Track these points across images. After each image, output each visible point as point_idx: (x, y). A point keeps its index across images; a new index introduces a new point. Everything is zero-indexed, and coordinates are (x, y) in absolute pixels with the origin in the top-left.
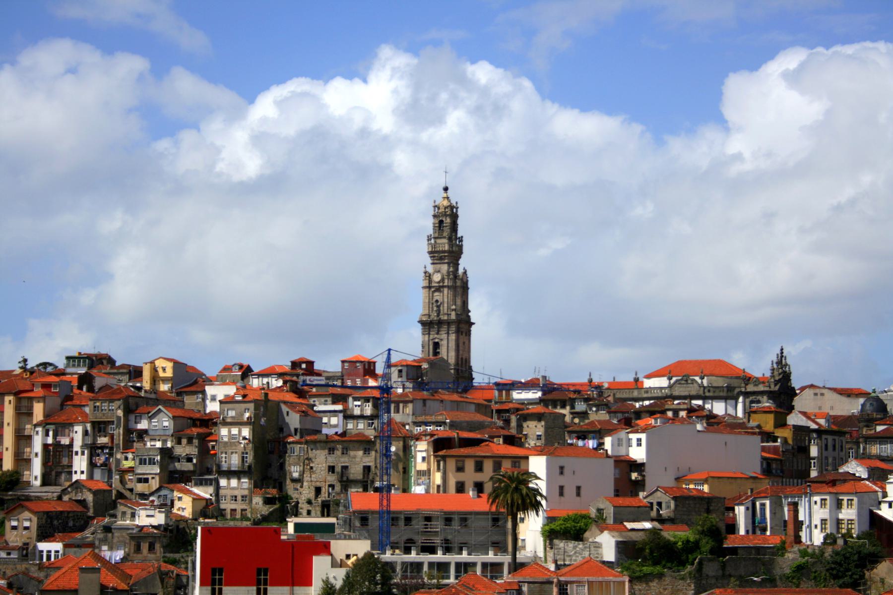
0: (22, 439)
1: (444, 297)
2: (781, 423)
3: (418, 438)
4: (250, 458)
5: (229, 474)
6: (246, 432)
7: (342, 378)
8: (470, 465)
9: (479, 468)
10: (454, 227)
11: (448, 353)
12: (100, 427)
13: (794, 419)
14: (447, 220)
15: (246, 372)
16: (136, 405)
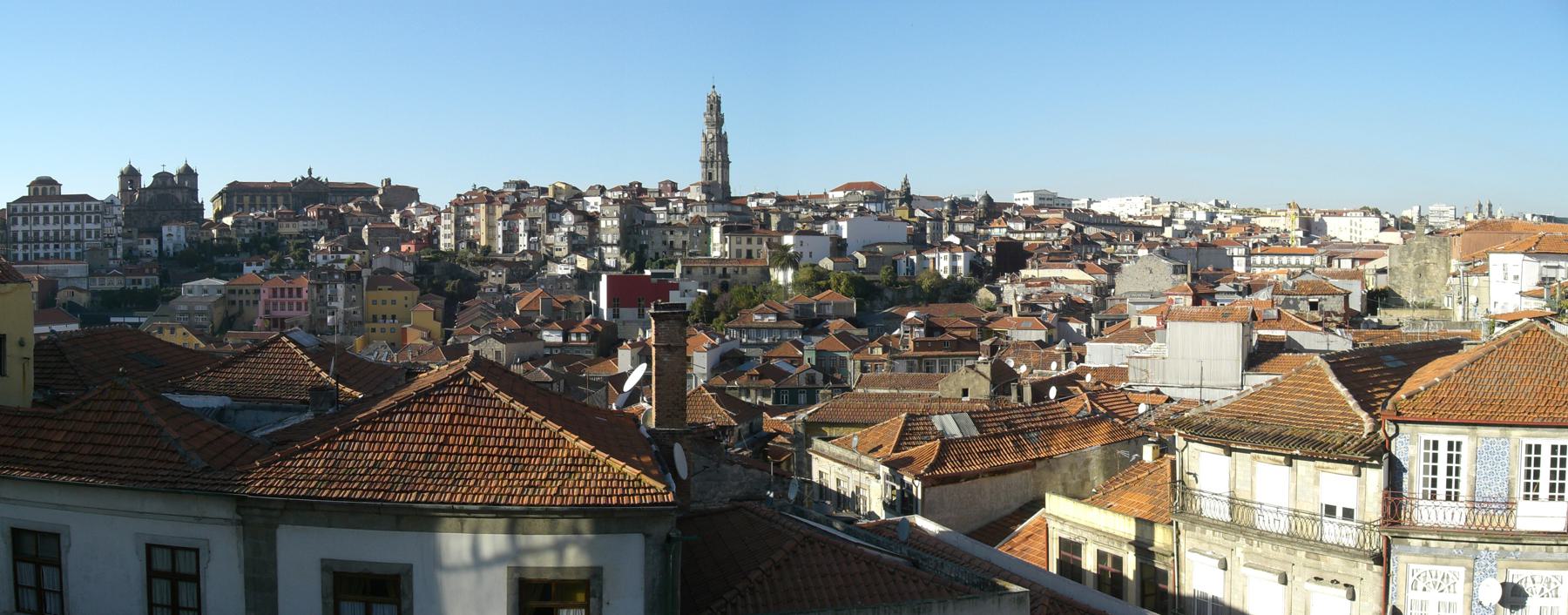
0: (490, 227)
1: (714, 147)
2: (912, 215)
3: (714, 224)
4: (618, 237)
5: (607, 245)
6: (616, 222)
7: (660, 192)
8: (744, 239)
9: (749, 241)
10: (719, 109)
11: (717, 178)
12: (532, 220)
13: (919, 213)
14: (715, 105)
15: (603, 190)
16: (554, 208)
